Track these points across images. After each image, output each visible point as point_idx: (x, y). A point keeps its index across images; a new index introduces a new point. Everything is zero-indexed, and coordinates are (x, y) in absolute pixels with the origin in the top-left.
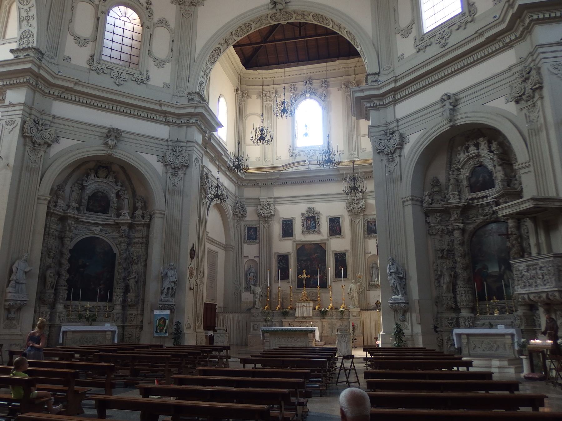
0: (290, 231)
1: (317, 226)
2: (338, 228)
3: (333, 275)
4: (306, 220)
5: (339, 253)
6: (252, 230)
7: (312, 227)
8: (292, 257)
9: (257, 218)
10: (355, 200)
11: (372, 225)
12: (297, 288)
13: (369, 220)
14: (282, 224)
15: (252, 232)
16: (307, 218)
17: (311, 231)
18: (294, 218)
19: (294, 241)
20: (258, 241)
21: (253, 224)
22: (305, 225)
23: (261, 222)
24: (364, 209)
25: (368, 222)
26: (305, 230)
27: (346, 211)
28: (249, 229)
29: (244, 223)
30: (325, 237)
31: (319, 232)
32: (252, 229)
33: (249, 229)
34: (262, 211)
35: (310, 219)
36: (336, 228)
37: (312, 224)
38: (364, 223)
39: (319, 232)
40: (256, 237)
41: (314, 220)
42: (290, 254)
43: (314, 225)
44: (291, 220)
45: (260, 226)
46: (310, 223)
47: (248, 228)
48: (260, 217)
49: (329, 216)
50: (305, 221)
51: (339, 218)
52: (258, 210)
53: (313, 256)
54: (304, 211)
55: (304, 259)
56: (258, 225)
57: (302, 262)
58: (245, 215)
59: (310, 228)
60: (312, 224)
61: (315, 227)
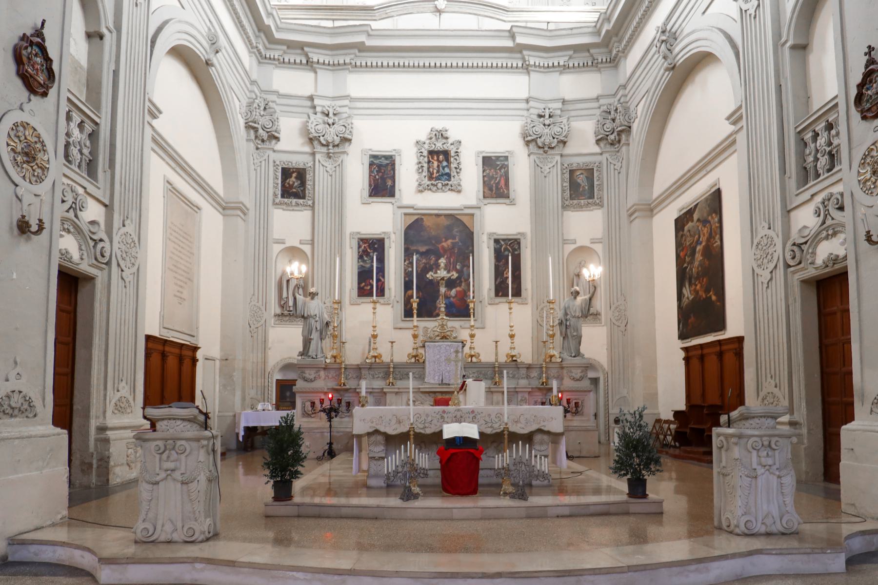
0: (389, 183)
1: (454, 173)
2: (502, 183)
4: (428, 157)
5: (504, 240)
6: (294, 175)
7: (442, 175)
8: (393, 245)
9: (307, 149)
10: (547, 116)
11: (581, 179)
12: (405, 316)
14: (371, 165)
16: (431, 153)
17: (440, 185)
19: (399, 207)
20: (310, 203)
21: (298, 161)
22: (425, 169)
23: (318, 157)
24: (566, 140)
25: (572, 172)
26: (426, 182)
27: (520, 143)
28: (286, 173)
29: (273, 156)
30: (473, 202)
32: (293, 172)
33: (286, 173)
34: (319, 127)
36: (500, 180)
37: (443, 169)
38: (563, 174)
40: (304, 191)
42: (389, 238)
43: (447, 170)
46: (438, 166)
47: (283, 169)
48: (316, 143)
49: (481, 152)
50: (426, 159)
51: (506, 158)
52: (312, 127)
53: (444, 244)
54: (423, 137)
55: (423, 249)
56: (310, 165)
58: (276, 134)
59: (438, 179)
60: (443, 169)
61: (449, 176)
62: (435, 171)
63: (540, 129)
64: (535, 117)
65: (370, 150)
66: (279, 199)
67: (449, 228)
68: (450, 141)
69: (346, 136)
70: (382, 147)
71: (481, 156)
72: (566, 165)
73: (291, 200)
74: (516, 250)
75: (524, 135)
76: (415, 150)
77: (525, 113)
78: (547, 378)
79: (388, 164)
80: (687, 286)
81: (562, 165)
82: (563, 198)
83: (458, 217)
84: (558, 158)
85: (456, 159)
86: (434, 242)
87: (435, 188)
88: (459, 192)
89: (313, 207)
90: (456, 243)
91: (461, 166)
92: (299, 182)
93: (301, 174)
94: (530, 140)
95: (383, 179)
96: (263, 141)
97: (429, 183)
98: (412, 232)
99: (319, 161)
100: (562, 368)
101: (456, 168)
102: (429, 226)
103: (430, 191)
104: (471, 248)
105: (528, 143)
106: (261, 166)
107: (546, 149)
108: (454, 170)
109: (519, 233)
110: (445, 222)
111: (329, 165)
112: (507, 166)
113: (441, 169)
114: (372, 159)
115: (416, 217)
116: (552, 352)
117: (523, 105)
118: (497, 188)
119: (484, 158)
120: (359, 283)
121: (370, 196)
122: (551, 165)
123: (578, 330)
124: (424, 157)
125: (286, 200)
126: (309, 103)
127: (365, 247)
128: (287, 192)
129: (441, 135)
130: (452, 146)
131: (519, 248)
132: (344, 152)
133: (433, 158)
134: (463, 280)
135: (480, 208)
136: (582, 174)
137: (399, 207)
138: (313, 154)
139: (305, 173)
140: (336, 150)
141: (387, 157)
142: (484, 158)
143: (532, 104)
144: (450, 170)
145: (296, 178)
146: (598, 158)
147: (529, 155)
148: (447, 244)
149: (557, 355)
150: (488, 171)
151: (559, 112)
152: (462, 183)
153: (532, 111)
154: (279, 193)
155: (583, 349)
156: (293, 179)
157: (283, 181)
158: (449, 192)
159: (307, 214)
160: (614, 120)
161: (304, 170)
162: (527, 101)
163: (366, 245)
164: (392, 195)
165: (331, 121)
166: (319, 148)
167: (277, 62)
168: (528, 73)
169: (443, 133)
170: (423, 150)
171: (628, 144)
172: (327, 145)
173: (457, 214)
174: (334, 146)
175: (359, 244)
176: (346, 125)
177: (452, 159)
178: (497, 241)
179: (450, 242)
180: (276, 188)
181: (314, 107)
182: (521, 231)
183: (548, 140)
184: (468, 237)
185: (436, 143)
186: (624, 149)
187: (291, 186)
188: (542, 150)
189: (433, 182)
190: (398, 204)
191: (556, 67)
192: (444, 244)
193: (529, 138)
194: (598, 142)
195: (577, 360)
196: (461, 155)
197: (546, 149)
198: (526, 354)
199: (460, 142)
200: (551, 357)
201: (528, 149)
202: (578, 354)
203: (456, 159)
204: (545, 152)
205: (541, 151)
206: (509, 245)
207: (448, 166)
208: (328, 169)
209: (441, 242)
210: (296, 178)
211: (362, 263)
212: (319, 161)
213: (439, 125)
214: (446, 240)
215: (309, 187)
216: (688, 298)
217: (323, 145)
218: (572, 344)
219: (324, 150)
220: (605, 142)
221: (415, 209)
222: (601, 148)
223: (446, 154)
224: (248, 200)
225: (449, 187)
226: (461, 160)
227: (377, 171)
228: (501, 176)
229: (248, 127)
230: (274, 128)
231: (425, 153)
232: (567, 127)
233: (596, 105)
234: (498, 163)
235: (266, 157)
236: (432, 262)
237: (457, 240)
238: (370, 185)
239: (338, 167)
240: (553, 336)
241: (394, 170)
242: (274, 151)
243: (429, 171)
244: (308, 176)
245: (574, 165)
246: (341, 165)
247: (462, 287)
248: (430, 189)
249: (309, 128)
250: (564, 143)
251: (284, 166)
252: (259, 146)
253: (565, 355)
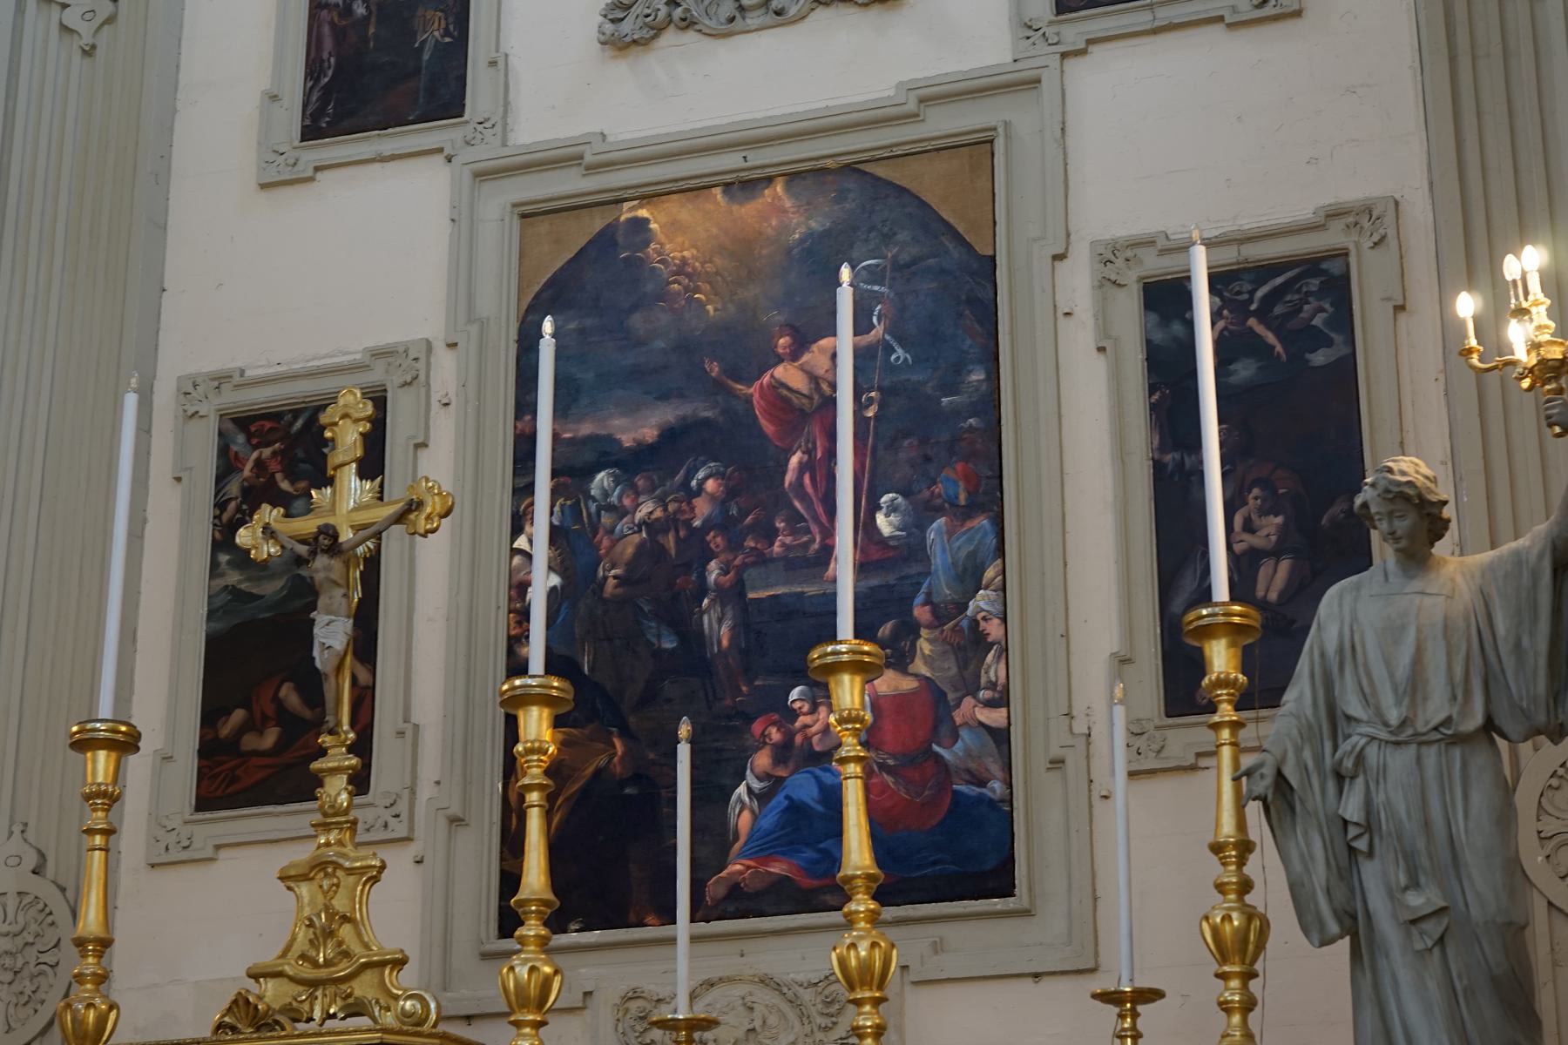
0: (432, 31)
3: (1123, 661)
19: (482, 175)
53: (787, 374)
57: (602, 478)
74: (1319, 340)
83: (880, 171)
86: (714, 369)
102: (682, 269)
103: (691, 36)
109: (1334, 214)
115: (596, 223)
120: (211, 715)
127: (259, 463)
131: (1343, 319)
134: (921, 613)
137: (482, 175)
163: (267, 452)
173: (892, 157)
175: (224, 451)
182: (1351, 192)
190: (487, 152)
206: (1262, 315)
211: (233, 578)
221: (593, 168)
236: (703, 509)
238: (313, 69)
247: (919, 666)
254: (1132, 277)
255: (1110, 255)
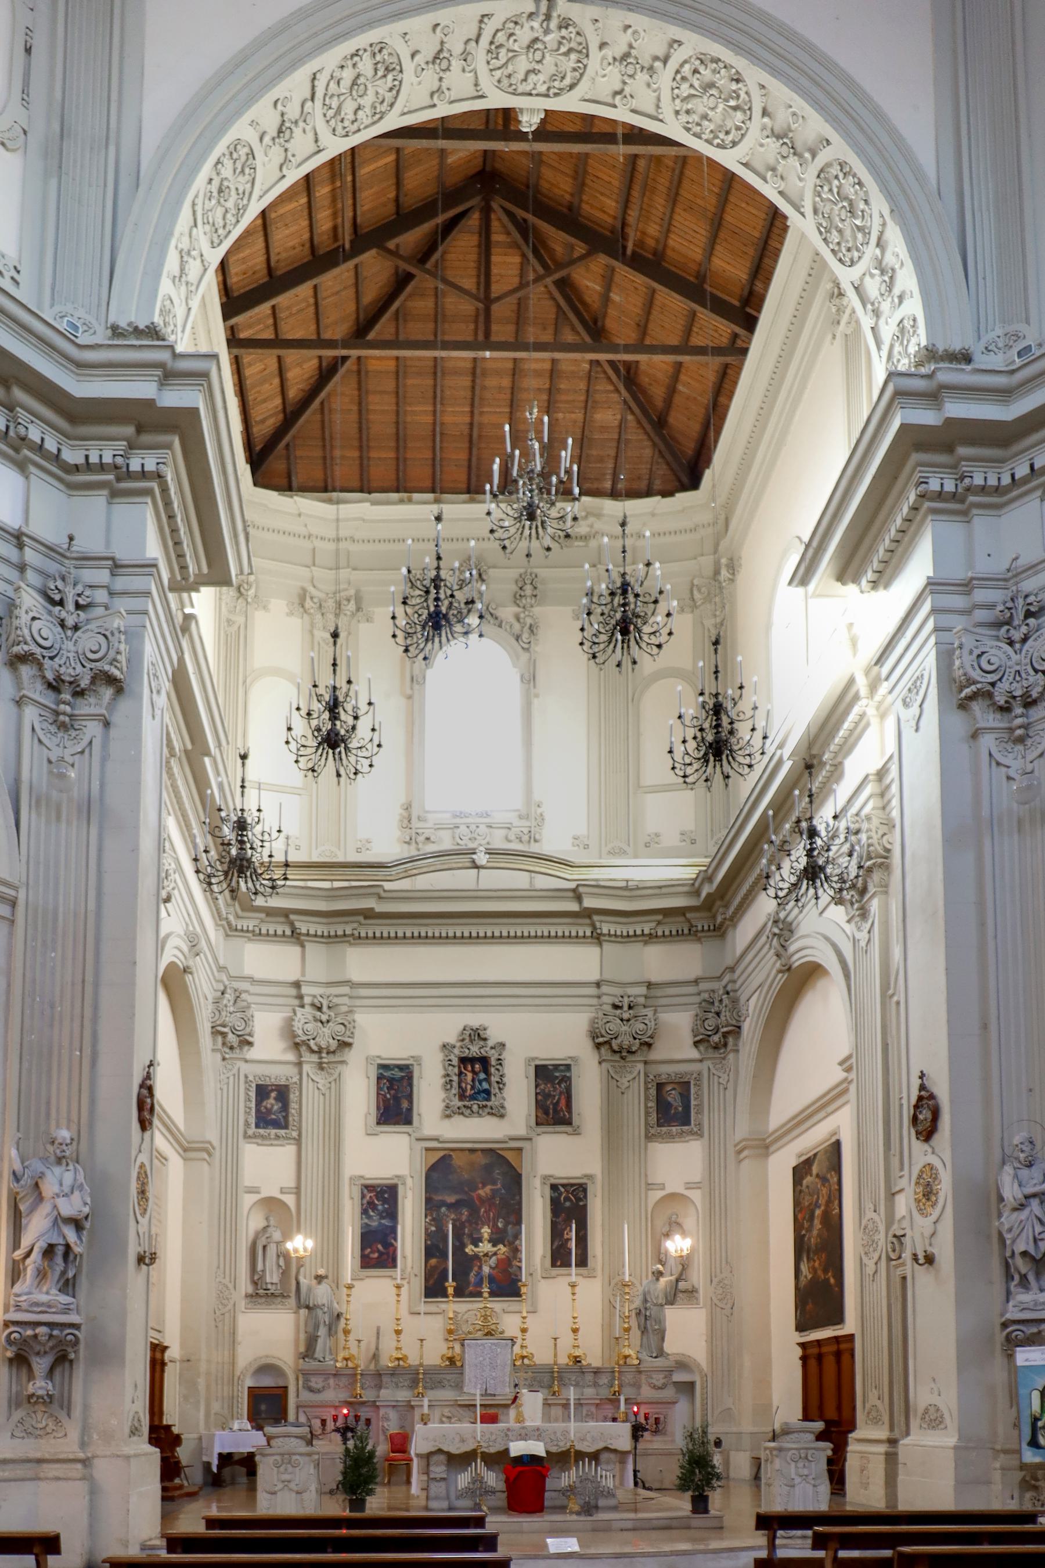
0: (405, 1105)
1: (495, 1090)
2: (563, 1104)
4: (459, 1067)
6: (273, 1095)
7: (479, 1092)
13: (663, 1079)
14: (380, 1078)
15: (271, 1102)
16: (464, 1060)
17: (475, 1108)
18: (418, 1059)
19: (417, 1140)
20: (295, 1134)
22: (455, 1084)
23: (306, 1068)
25: (660, 1086)
26: (456, 1103)
28: (262, 1092)
29: (245, 1068)
30: (521, 1131)
31: (499, 1113)
32: (272, 1090)
33: (262, 1092)
34: (309, 1027)
35: (473, 1067)
36: (559, 1099)
37: (480, 1084)
38: (647, 1089)
39: (499, 1113)
40: (286, 1118)
41: (486, 1071)
42: (404, 1184)
43: (485, 1085)
44: (407, 1067)
45: (301, 1079)
46: (473, 1080)
47: (258, 1086)
48: (303, 1049)
49: (534, 1059)
50: (456, 1070)
51: (568, 1067)
52: (298, 1027)
53: (481, 1192)
54: (452, 1039)
55: (451, 1199)
57: (443, 1209)
59: (472, 1098)
60: (480, 1084)
61: (488, 1092)
62: (469, 1087)
63: (615, 1026)
64: (608, 1008)
65: (378, 1057)
66: (252, 1130)
67: (488, 1169)
68: (490, 1043)
69: (347, 1039)
70: (395, 1052)
71: (533, 1064)
72: (652, 1077)
73: (268, 1131)
75: (594, 1035)
76: (440, 1056)
77: (595, 1001)
78: (620, 1386)
79: (402, 1078)
80: (805, 1259)
81: (646, 1075)
82: (647, 1124)
84: (640, 1066)
85: (498, 1070)
87: (469, 1111)
88: (502, 1116)
89: (298, 1141)
90: (498, 1190)
91: (505, 1080)
92: (280, 1105)
93: (283, 1093)
94: (601, 1042)
95: (397, 1099)
96: (232, 1048)
97: (460, 1104)
98: (435, 1175)
99: (308, 1075)
100: (640, 1372)
101: (498, 1082)
102: (459, 1167)
103: (461, 1117)
104: (517, 1198)
105: (598, 1046)
106: (228, 1084)
107: (623, 1053)
108: (496, 1085)
110: (481, 1160)
111: (321, 1079)
112: (569, 1079)
113: (477, 1083)
114: (381, 1071)
115: (441, 1154)
116: (627, 1351)
117: (593, 991)
118: (555, 1111)
119: (537, 1067)
121: (378, 1123)
122: (632, 1076)
123: (660, 1321)
124: (454, 1066)
125: (261, 1131)
126: (293, 992)
128: (264, 1120)
129: (477, 1035)
130: (493, 1051)
132: (343, 1062)
133: (465, 1069)
135: (530, 1139)
136: (674, 1089)
138: (299, 1064)
139: (288, 1090)
140: (332, 1058)
141: (401, 1068)
142: (537, 1067)
143: (605, 989)
144: (490, 1085)
145: (275, 1099)
146: (695, 1067)
147: (600, 1063)
148: (484, 1192)
149: (634, 1356)
150: (542, 1087)
151: (642, 1000)
152: (506, 1104)
153: (606, 999)
154: (252, 1120)
155: (668, 1347)
156: (272, 1101)
157: (258, 1104)
158: (489, 1117)
159: (290, 1150)
160: (718, 1014)
161: (287, 1086)
162: (598, 985)
164: (409, 1122)
165: (324, 1018)
166: (307, 1057)
167: (250, 935)
168: (600, 944)
169: (481, 1033)
170: (452, 1057)
171: (737, 1051)
172: (319, 1052)
173: (500, 1149)
174: (328, 1053)
176: (346, 1023)
177: (493, 1070)
178: (554, 1187)
179: (488, 1188)
180: (247, 1113)
181: (300, 997)
183: (626, 1041)
184: (515, 1180)
185: (470, 1047)
186: (731, 1056)
187: (269, 1111)
188: (618, 1055)
189: (467, 1103)
190: (418, 1135)
191: (639, 936)
192: (481, 1192)
193: (601, 1040)
194: (696, 1044)
195: (660, 1362)
196: (506, 1063)
197: (624, 1054)
198: (594, 1355)
199: (504, 1045)
200: (626, 1357)
201: (599, 1053)
202: (661, 1353)
203: (498, 1070)
204: (623, 1058)
205: (617, 1057)
207: (487, 1080)
208: (320, 1086)
209: (476, 1189)
210: (275, 1099)
212: (308, 1075)
213: (474, 1020)
214: (484, 1185)
215: (293, 1111)
216: (806, 1277)
217: (313, 1052)
218: (653, 1339)
219: (315, 1058)
220: (706, 1044)
222: (700, 1052)
223: (484, 1061)
224: (212, 1135)
225: (488, 1110)
226: (506, 1071)
227: (388, 1088)
228: (561, 1093)
229: (215, 1032)
230: (248, 1030)
231: (455, 1062)
232: (653, 1023)
233: (692, 989)
234: (557, 1074)
235: (235, 1071)
236: (464, 1218)
237: (499, 1186)
238: (378, 1108)
239: (333, 1084)
240: (627, 1330)
241: (411, 1085)
242: (246, 1061)
243: (460, 1087)
244: (292, 1096)
245: (663, 1077)
246: (338, 1080)
248: (462, 1114)
249: (295, 1029)
250: (649, 1045)
251: (260, 1083)
252: (227, 1056)
253: (644, 1356)
254: (548, 1183)
255: (545, 1178)
